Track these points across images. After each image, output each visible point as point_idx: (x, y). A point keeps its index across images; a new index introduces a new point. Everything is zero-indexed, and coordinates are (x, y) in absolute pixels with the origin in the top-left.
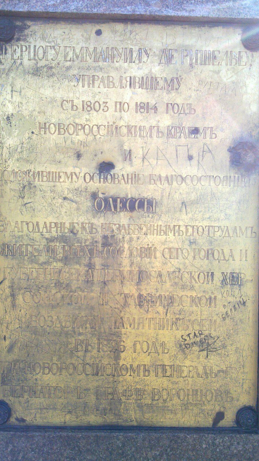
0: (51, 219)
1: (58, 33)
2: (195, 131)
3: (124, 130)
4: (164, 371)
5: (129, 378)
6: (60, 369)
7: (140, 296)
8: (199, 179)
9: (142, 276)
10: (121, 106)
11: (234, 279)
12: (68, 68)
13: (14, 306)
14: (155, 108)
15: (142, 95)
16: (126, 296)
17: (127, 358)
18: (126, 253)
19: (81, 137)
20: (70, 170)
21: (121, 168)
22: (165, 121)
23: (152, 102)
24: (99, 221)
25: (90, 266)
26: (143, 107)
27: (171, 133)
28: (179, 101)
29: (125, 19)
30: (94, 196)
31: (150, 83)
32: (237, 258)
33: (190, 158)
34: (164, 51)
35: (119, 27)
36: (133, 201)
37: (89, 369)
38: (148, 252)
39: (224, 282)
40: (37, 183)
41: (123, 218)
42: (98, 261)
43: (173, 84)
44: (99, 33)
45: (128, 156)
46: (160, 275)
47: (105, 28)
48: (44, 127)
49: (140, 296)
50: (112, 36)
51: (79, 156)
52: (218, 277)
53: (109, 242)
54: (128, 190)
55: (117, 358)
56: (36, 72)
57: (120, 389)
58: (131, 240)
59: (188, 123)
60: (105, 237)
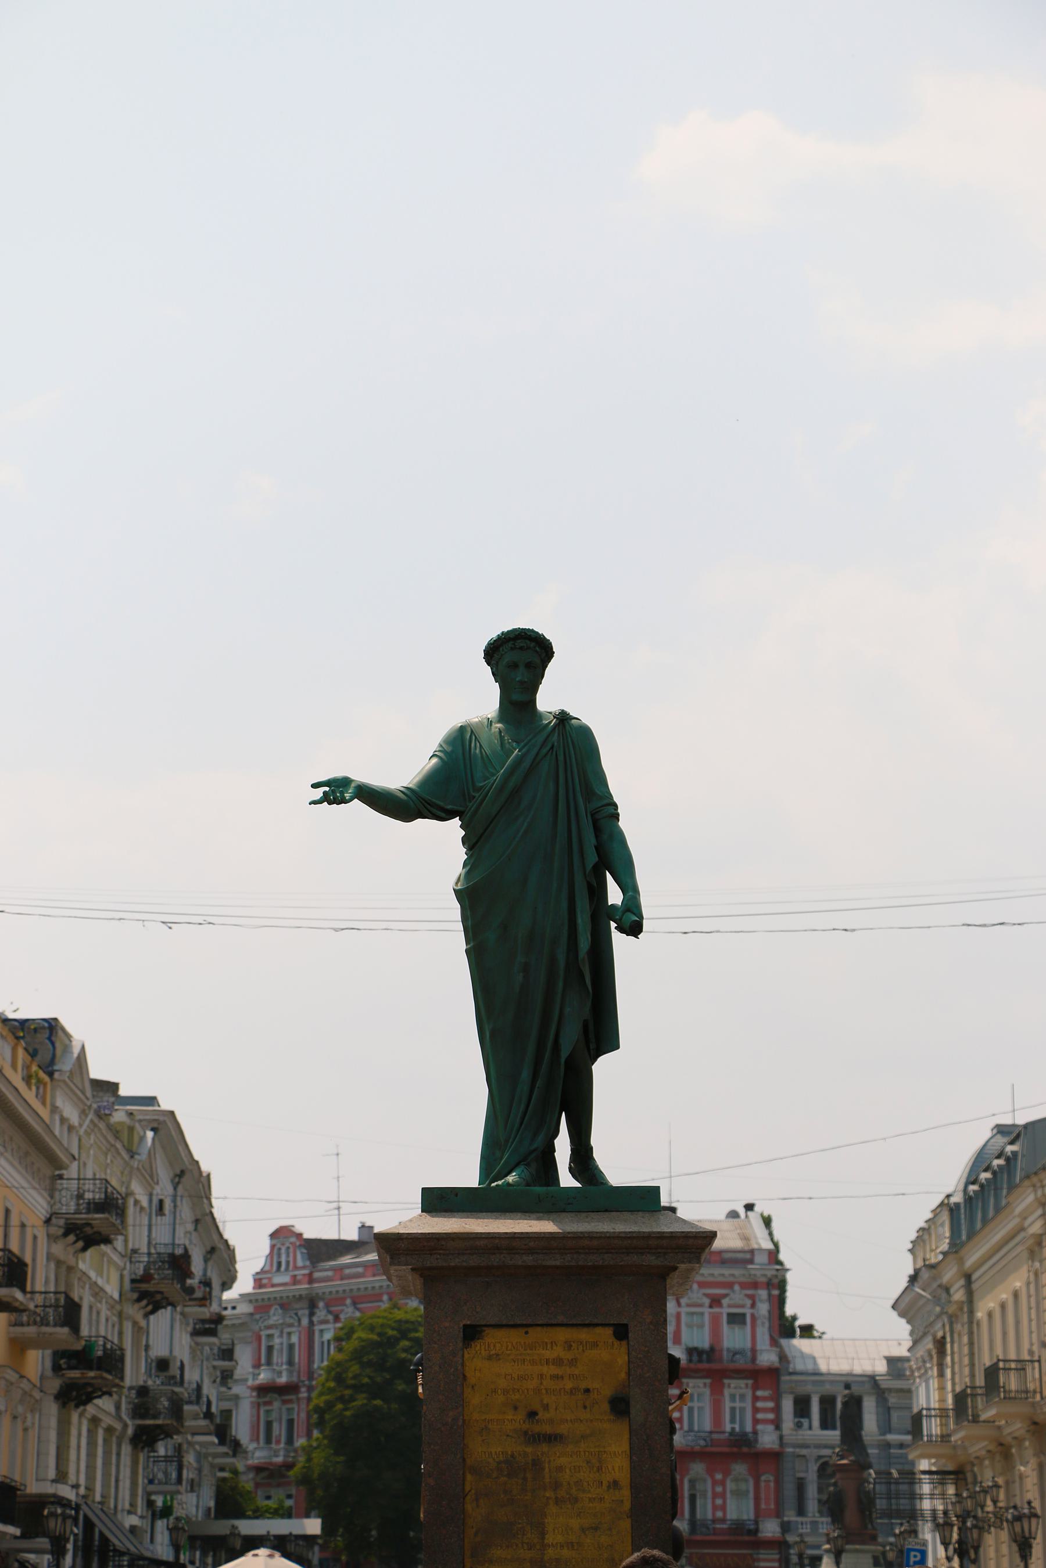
0: (499, 1449)
1: (501, 1334)
2: (587, 1391)
3: (544, 1391)
4: (573, 1546)
5: (550, 1552)
6: (508, 1547)
7: (556, 1498)
8: (591, 1421)
9: (556, 1485)
10: (541, 1376)
11: (615, 1484)
12: (509, 1355)
13: (478, 1506)
14: (562, 1377)
15: (553, 1370)
16: (548, 1498)
17: (550, 1539)
18: (547, 1470)
19: (517, 1396)
20: (510, 1417)
21: (542, 1415)
22: (569, 1385)
23: (560, 1374)
24: (529, 1450)
25: (525, 1479)
26: (555, 1377)
27: (572, 1392)
28: (577, 1372)
29: (542, 1325)
30: (526, 1433)
31: (558, 1362)
32: (617, 1469)
33: (585, 1407)
34: (566, 1342)
35: (539, 1329)
36: (550, 1436)
37: (525, 1546)
38: (560, 1469)
39: (609, 1487)
40: (490, 1426)
41: (545, 1447)
42: (529, 1475)
43: (573, 1362)
44: (526, 1333)
45: (546, 1407)
46: (569, 1484)
47: (530, 1330)
48: (495, 1391)
49: (556, 1498)
50: (536, 1334)
51: (516, 1408)
52: (605, 1484)
53: (537, 1464)
54: (548, 1429)
55: (543, 1538)
56: (489, 1358)
57: (546, 1558)
58: (550, 1461)
59: (583, 1385)
60: (533, 1460)
